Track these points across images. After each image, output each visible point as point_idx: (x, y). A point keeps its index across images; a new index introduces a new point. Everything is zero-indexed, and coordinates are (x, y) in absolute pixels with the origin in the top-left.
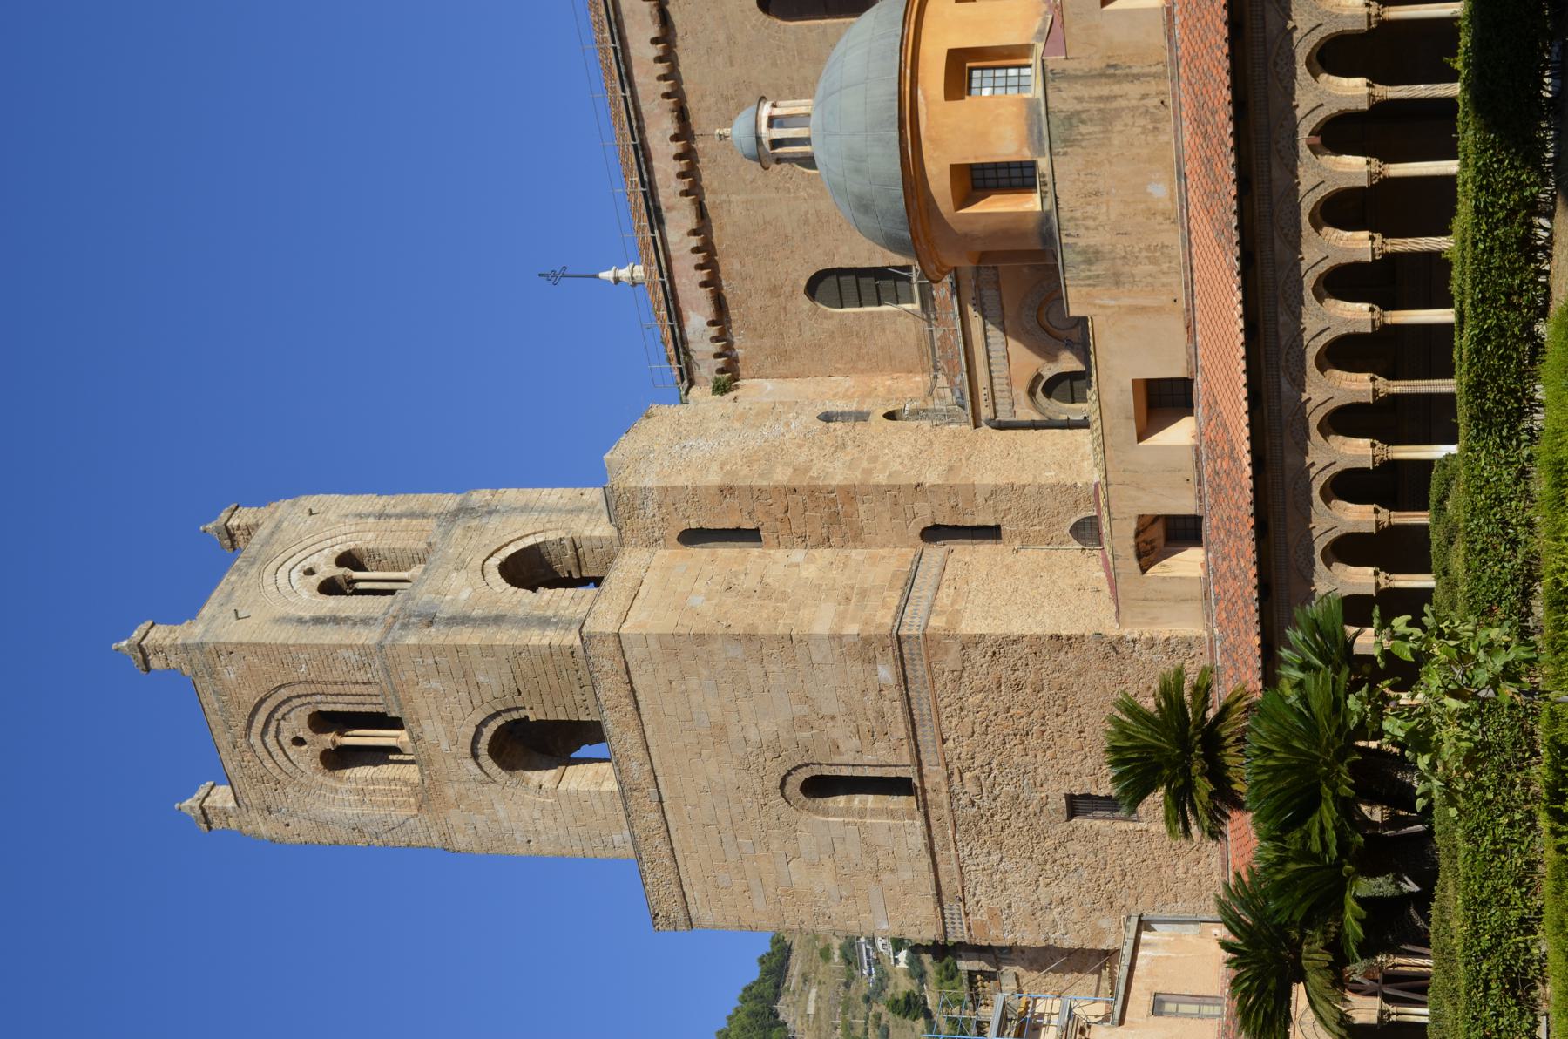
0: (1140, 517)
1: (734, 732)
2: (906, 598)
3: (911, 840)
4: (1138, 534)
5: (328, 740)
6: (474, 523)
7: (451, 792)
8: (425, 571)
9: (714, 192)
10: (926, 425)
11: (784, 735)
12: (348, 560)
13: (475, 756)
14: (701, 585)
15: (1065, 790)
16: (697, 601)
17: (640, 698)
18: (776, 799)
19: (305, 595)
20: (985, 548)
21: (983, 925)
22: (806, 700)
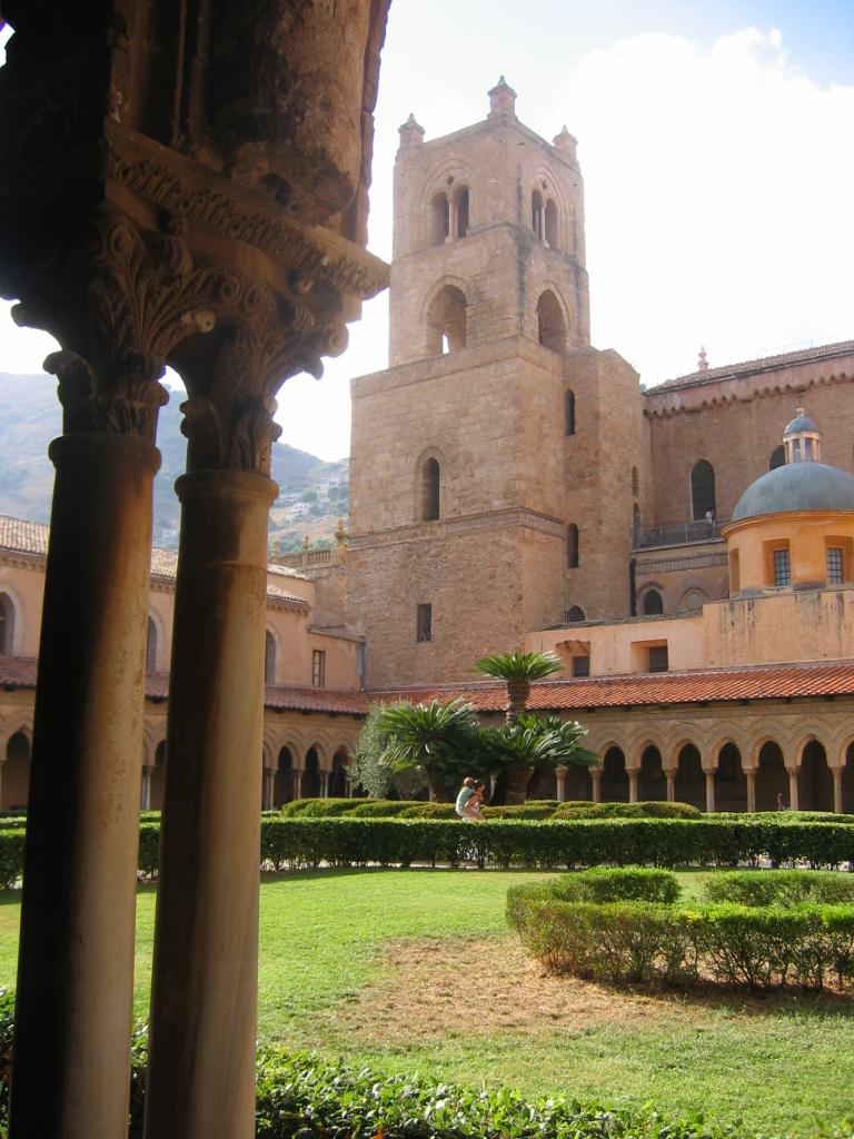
0: (589, 643)
1: (463, 421)
2: (538, 514)
3: (404, 519)
4: (578, 641)
5: (450, 196)
6: (572, 276)
7: (423, 265)
8: (546, 249)
9: (757, 408)
10: (632, 526)
11: (462, 449)
12: (551, 206)
13: (444, 278)
14: (544, 402)
15: (434, 604)
16: (536, 400)
17: (482, 370)
18: (425, 444)
19: (532, 182)
20: (562, 557)
21: (358, 559)
22: (482, 461)
